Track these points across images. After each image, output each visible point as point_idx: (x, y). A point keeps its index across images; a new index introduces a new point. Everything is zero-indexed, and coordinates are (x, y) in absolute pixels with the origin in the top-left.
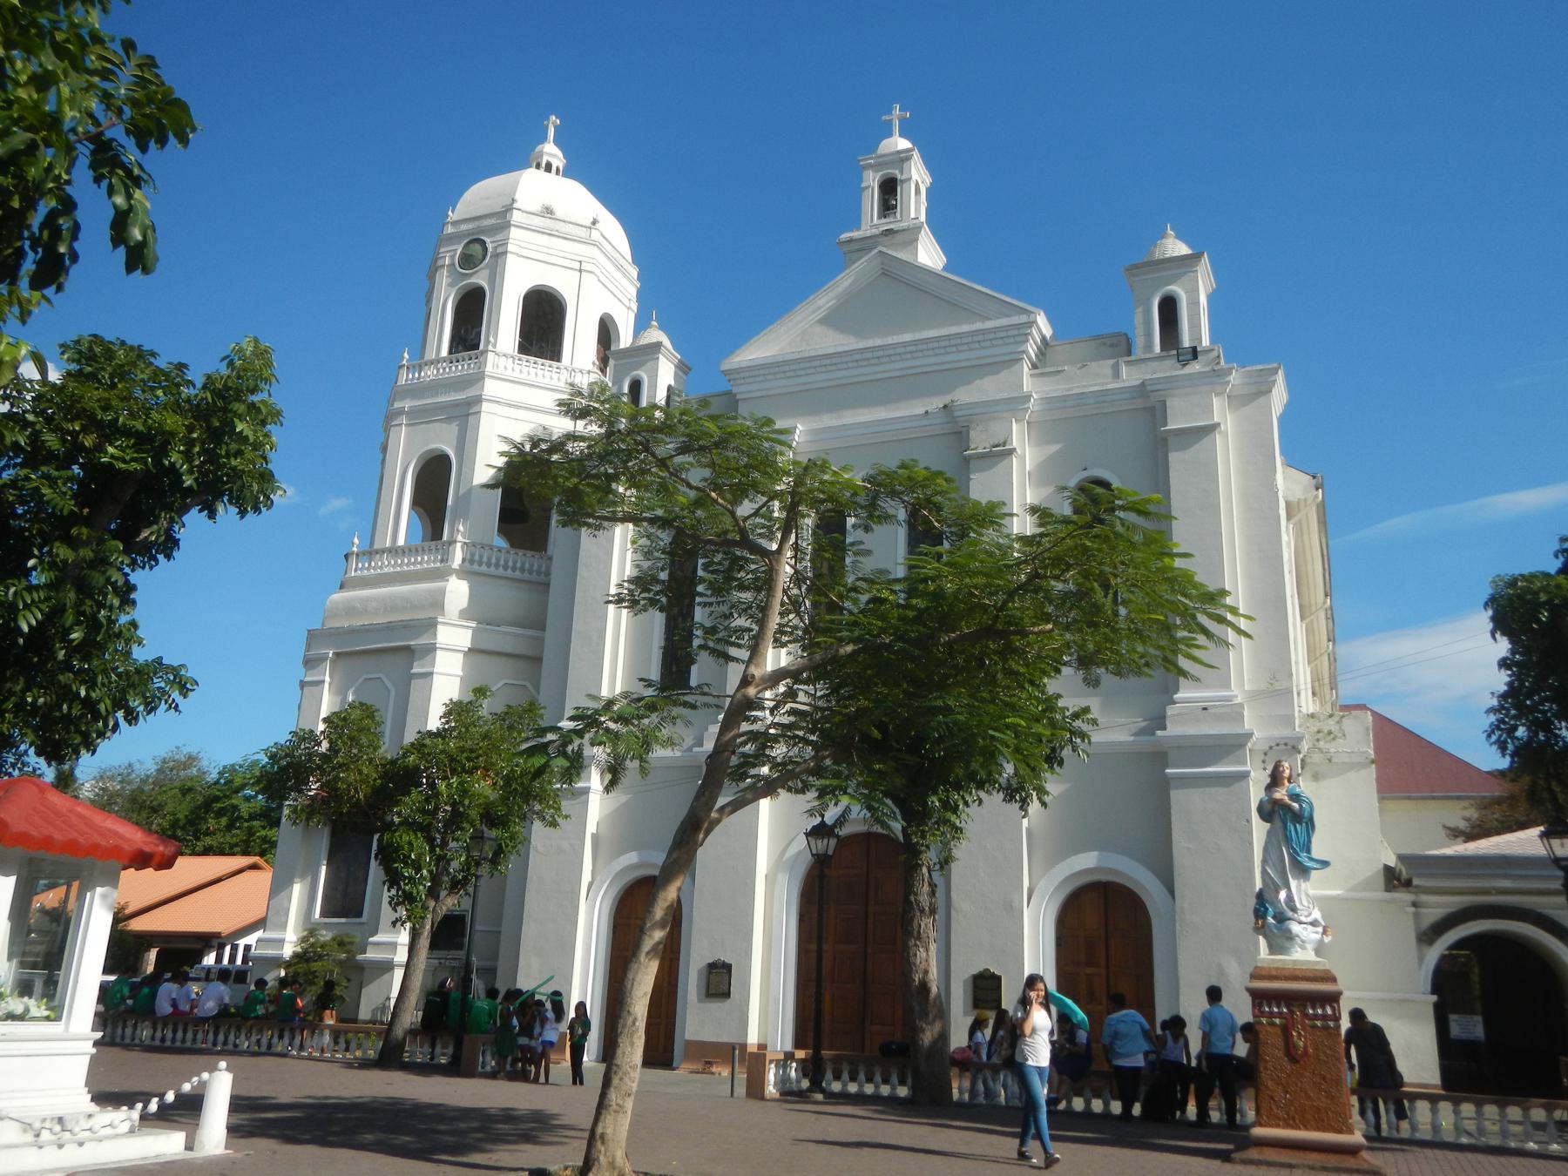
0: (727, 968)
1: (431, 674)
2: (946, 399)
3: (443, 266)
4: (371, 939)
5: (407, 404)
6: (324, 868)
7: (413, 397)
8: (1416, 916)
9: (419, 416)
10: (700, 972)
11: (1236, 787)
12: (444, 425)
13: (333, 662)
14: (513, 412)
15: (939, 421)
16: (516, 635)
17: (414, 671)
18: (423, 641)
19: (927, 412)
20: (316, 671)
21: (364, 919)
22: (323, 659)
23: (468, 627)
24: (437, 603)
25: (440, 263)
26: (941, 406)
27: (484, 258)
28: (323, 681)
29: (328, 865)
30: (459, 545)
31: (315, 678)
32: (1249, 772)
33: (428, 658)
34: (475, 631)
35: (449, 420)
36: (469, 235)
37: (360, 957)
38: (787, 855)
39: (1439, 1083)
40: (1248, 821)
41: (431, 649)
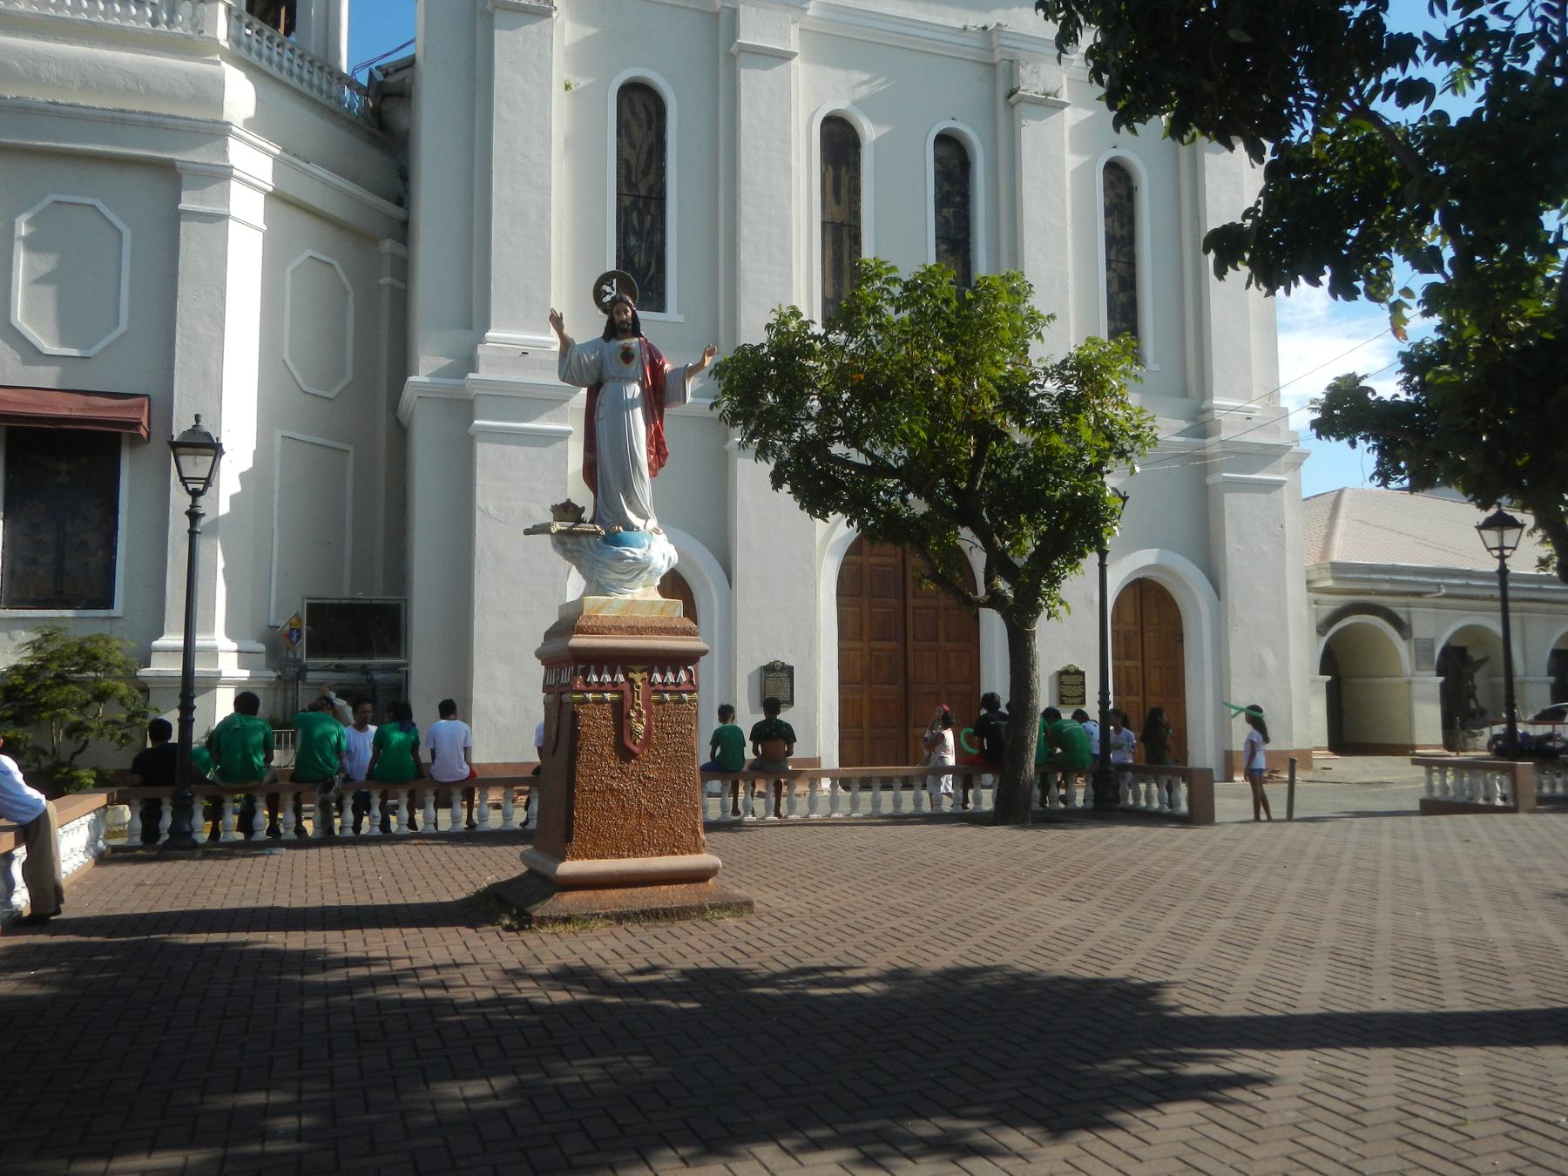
0: (789, 671)
1: (224, 218)
2: (991, 20)
4: (155, 643)
8: (1316, 610)
10: (750, 677)
11: (1273, 495)
15: (974, 43)
16: (325, 182)
17: (182, 206)
19: (965, 28)
21: (118, 610)
23: (268, 153)
24: (212, 95)
26: (980, 26)
32: (1284, 482)
33: (214, 188)
34: (276, 159)
37: (144, 672)
38: (834, 539)
39: (1326, 745)
40: (1282, 527)
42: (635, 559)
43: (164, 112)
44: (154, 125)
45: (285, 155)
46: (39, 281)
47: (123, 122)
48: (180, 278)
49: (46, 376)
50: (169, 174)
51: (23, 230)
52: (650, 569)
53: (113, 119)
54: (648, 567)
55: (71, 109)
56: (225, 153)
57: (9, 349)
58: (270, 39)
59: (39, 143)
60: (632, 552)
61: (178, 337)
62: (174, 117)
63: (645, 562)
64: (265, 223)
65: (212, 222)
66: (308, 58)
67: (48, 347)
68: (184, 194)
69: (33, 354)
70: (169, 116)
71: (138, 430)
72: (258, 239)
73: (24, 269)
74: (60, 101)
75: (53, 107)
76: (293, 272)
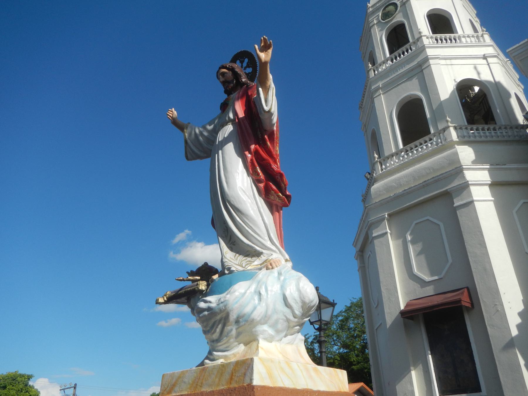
1: (472, 202)
3: (374, 25)
5: (380, 84)
6: (430, 356)
7: (382, 80)
9: (387, 88)
12: (408, 83)
13: (388, 221)
14: (448, 62)
16: (518, 169)
18: (456, 183)
20: (378, 228)
22: (383, 219)
24: (455, 159)
25: (371, 25)
27: (396, 9)
28: (386, 233)
29: (431, 354)
30: (452, 129)
31: (380, 233)
33: (465, 193)
34: (489, 170)
35: (410, 79)
36: (383, 5)
41: (466, 186)
42: (209, 309)
43: (438, 174)
44: (437, 181)
45: (493, 167)
46: (418, 254)
47: (427, 185)
48: (463, 234)
49: (430, 291)
50: (448, 196)
51: (409, 238)
52: (233, 317)
53: (423, 186)
54: (226, 318)
55: (410, 189)
56: (464, 177)
57: (415, 284)
58: (477, 130)
59: (405, 206)
60: (206, 302)
61: (470, 258)
62: (442, 174)
63: (221, 311)
64: (493, 197)
65: (468, 206)
66: (503, 127)
67: (427, 278)
68: (455, 200)
69: (423, 283)
70: (440, 175)
71: (461, 303)
72: (492, 205)
73: (413, 252)
74: (406, 189)
75: (405, 192)
76: (516, 212)
